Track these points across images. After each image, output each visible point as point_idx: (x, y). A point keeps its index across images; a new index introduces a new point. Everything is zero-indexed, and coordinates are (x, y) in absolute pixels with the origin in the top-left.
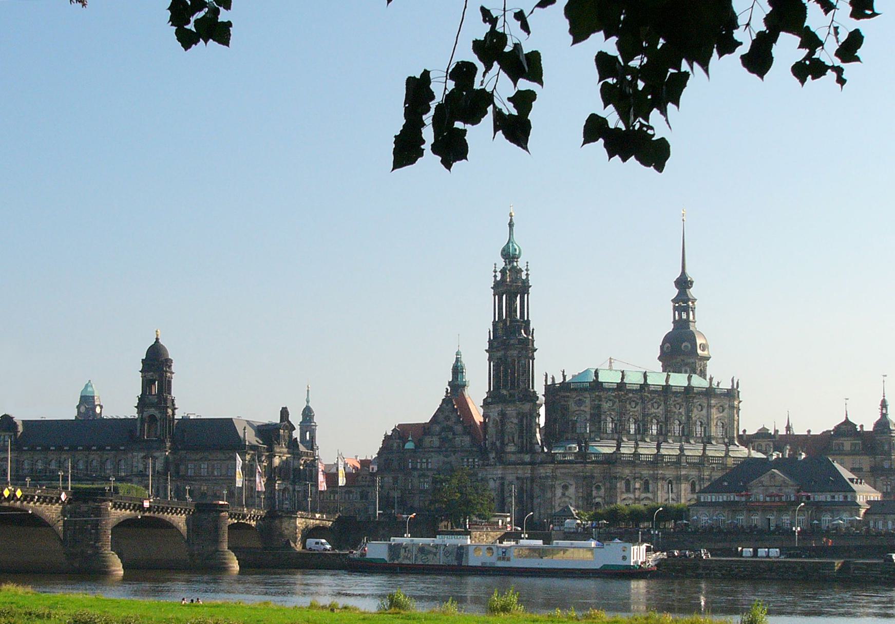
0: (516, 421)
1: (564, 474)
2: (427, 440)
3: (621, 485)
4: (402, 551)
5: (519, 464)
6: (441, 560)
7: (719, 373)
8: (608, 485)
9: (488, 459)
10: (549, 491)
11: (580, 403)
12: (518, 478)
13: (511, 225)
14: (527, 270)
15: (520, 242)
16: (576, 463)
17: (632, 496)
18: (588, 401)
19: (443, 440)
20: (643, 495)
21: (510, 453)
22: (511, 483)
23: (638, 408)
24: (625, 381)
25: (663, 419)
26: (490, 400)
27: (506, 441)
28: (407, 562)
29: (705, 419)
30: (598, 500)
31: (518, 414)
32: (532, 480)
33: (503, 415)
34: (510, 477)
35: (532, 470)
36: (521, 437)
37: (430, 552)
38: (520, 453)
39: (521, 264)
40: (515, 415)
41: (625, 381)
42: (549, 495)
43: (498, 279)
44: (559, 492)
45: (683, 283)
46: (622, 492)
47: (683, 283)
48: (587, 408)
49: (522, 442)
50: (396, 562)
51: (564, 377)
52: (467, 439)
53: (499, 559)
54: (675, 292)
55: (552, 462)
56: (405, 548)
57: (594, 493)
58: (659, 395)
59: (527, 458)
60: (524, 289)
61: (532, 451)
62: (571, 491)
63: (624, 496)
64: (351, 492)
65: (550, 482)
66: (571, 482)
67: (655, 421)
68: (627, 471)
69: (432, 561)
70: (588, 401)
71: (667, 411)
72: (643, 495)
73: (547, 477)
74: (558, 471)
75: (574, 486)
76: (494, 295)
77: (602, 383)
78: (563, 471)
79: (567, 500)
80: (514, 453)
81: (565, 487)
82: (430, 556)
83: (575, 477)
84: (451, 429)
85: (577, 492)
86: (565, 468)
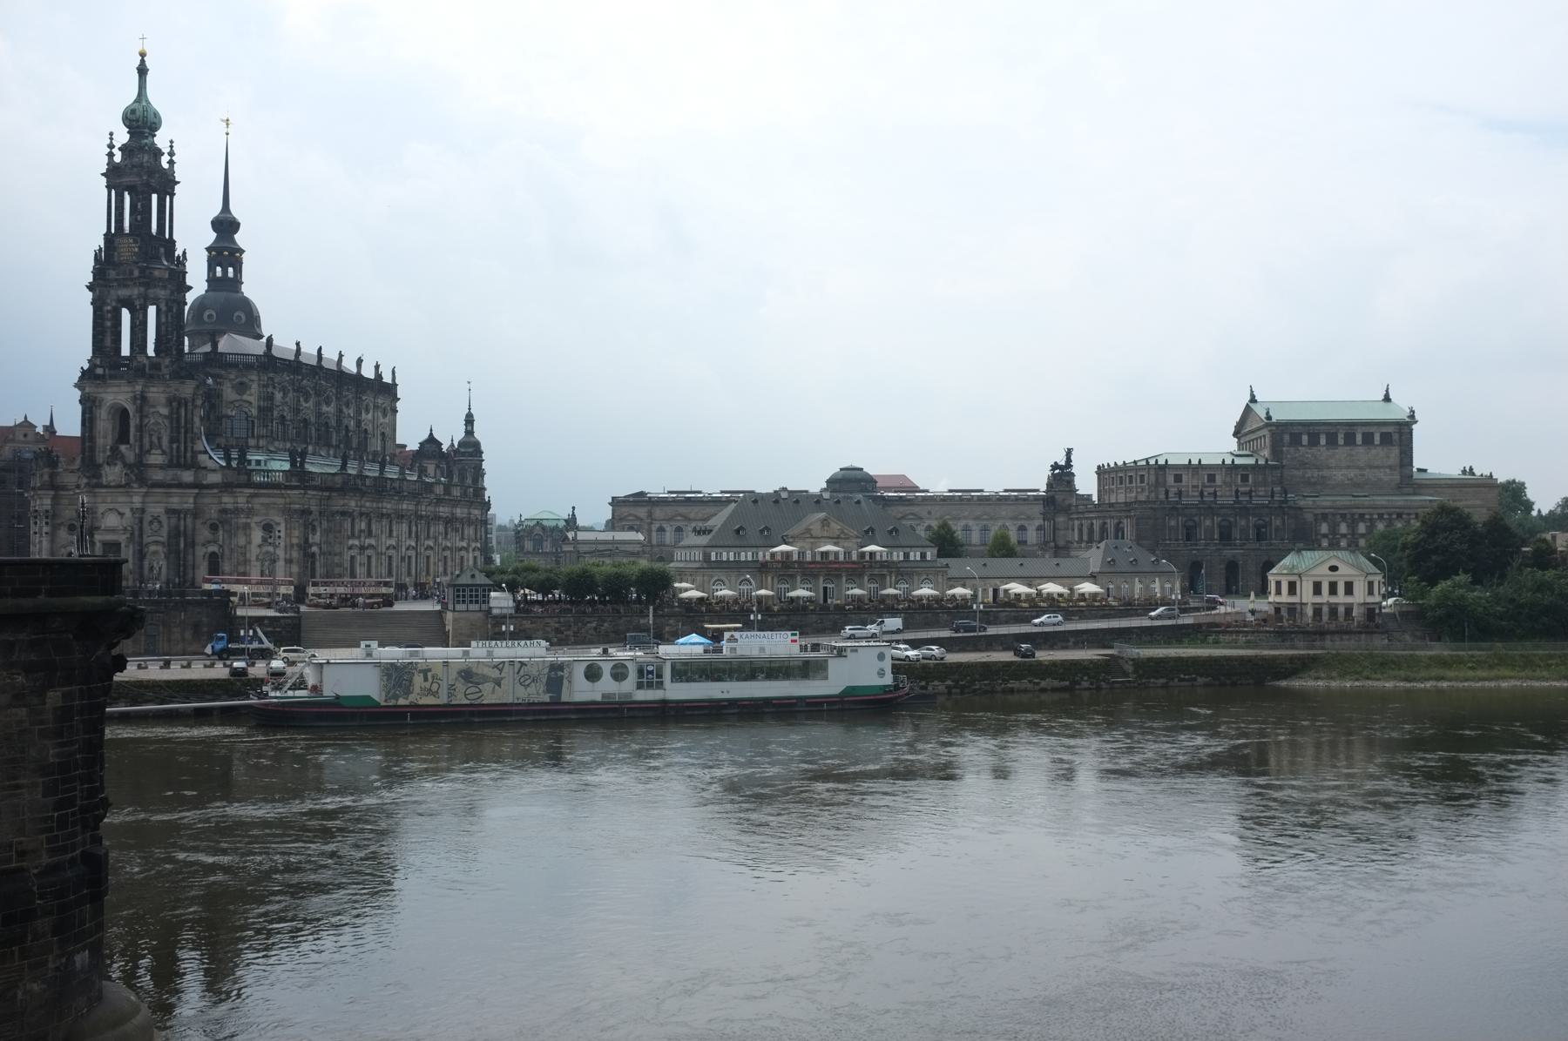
0: (164, 411)
3: (347, 525)
4: (418, 680)
5: (170, 486)
6: (509, 693)
10: (241, 532)
11: (242, 388)
12: (170, 512)
13: (142, 71)
14: (171, 154)
15: (157, 99)
16: (287, 487)
18: (255, 386)
21: (155, 466)
22: (156, 519)
23: (310, 404)
25: (333, 422)
27: (147, 447)
28: (429, 700)
31: (170, 401)
32: (196, 513)
33: (142, 400)
35: (196, 496)
36: (172, 441)
37: (486, 679)
40: (163, 401)
42: (242, 541)
43: (118, 158)
45: (225, 226)
47: (225, 226)
48: (252, 396)
50: (402, 702)
53: (640, 686)
55: (249, 484)
56: (425, 672)
59: (188, 476)
60: (167, 184)
61: (194, 465)
66: (277, 519)
68: (353, 503)
69: (490, 695)
70: (255, 386)
74: (256, 500)
76: (109, 187)
79: (271, 549)
80: (161, 467)
82: (487, 687)
83: (288, 512)
86: (268, 496)
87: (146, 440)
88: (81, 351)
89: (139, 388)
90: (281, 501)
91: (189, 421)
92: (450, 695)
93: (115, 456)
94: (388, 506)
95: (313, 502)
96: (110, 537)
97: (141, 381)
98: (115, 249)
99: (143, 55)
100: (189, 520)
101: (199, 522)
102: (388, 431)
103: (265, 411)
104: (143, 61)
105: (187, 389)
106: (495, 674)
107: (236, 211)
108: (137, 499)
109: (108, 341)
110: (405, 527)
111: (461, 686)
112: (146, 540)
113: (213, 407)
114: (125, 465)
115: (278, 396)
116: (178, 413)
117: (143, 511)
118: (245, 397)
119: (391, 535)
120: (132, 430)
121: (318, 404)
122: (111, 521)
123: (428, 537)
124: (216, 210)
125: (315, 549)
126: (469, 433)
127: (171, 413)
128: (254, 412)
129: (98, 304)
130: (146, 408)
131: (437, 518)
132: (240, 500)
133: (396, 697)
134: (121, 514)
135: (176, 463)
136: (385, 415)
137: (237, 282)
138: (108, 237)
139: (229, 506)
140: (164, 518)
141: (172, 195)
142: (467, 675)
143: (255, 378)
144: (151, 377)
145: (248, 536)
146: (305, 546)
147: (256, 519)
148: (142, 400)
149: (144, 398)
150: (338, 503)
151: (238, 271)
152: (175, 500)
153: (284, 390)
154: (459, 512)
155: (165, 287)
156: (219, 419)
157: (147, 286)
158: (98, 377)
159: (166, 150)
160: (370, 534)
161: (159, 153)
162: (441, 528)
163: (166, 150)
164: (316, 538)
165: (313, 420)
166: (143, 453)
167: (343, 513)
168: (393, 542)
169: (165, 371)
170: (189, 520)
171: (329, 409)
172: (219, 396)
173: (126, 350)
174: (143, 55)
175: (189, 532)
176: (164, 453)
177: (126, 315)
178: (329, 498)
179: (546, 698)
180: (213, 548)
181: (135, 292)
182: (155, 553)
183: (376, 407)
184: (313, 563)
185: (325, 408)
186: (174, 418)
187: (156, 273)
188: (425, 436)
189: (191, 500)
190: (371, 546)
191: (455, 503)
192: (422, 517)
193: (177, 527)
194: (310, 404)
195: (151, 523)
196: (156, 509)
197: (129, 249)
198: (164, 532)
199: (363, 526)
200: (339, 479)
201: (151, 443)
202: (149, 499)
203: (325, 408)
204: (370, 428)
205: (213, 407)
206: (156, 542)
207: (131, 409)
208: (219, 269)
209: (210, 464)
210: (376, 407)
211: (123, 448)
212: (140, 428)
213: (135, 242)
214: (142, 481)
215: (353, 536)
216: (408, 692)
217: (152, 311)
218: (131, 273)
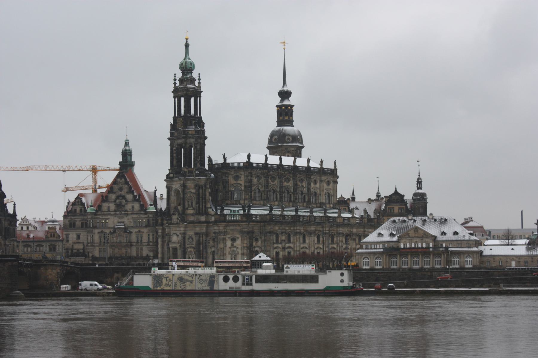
1: (233, 230)
2: (105, 206)
5: (196, 223)
7: (311, 157)
8: (263, 238)
9: (171, 220)
10: (221, 242)
11: (237, 178)
12: (196, 234)
13: (187, 46)
14: (199, 79)
15: (193, 57)
16: (242, 222)
17: (280, 246)
18: (243, 177)
19: (119, 207)
20: (287, 245)
21: (190, 214)
22: (191, 237)
23: (276, 182)
25: (292, 190)
26: (171, 175)
27: (187, 206)
29: (318, 190)
30: (257, 249)
32: (207, 234)
33: (184, 186)
34: (190, 233)
35: (207, 227)
36: (196, 204)
37: (187, 281)
39: (195, 75)
40: (193, 186)
41: (268, 162)
42: (222, 245)
43: (177, 85)
44: (229, 243)
48: (242, 181)
49: (199, 207)
51: (225, 159)
52: (137, 206)
55: (225, 221)
57: (254, 243)
58: (290, 173)
59: (203, 218)
60: (197, 93)
62: (238, 242)
63: (275, 245)
64: (42, 246)
65: (222, 237)
66: (238, 236)
67: (286, 192)
68: (277, 228)
69: (189, 287)
70: (243, 177)
71: (296, 185)
72: (287, 245)
73: (220, 233)
74: (228, 228)
75: (240, 238)
76: (174, 97)
77: (253, 163)
78: (232, 228)
79: (235, 249)
80: (193, 215)
81: (234, 240)
82: (188, 284)
83: (241, 232)
84: (124, 197)
85: (242, 243)
86: (233, 226)
87: (186, 204)
90: (239, 228)
92: (175, 286)
96: (174, 245)
98: (177, 123)
99: (187, 39)
100: (204, 237)
101: (208, 238)
106: (190, 279)
108: (182, 229)
111: (178, 283)
112: (187, 246)
115: (255, 180)
121: (281, 182)
122: (175, 238)
128: (243, 188)
131: (339, 234)
132: (221, 228)
133: (157, 287)
134: (178, 236)
135: (199, 212)
138: (175, 119)
139: (217, 231)
140: (194, 236)
141: (200, 97)
142: (181, 279)
143: (243, 173)
147: (228, 236)
150: (268, 228)
152: (197, 229)
153: (258, 177)
154: (355, 230)
155: (193, 138)
158: (171, 178)
159: (197, 78)
160: (289, 241)
163: (197, 78)
165: (278, 190)
166: (184, 209)
170: (204, 237)
172: (227, 182)
176: (194, 209)
178: (264, 226)
179: (208, 288)
180: (213, 249)
182: (191, 251)
183: (321, 181)
188: (393, 192)
189: (205, 229)
190: (290, 247)
192: (326, 233)
194: (276, 182)
195: (189, 239)
196: (190, 233)
198: (194, 243)
200: (268, 217)
201: (189, 205)
202: (188, 229)
203: (285, 184)
206: (191, 247)
207: (180, 190)
211: (179, 207)
215: (277, 242)
216: (161, 285)
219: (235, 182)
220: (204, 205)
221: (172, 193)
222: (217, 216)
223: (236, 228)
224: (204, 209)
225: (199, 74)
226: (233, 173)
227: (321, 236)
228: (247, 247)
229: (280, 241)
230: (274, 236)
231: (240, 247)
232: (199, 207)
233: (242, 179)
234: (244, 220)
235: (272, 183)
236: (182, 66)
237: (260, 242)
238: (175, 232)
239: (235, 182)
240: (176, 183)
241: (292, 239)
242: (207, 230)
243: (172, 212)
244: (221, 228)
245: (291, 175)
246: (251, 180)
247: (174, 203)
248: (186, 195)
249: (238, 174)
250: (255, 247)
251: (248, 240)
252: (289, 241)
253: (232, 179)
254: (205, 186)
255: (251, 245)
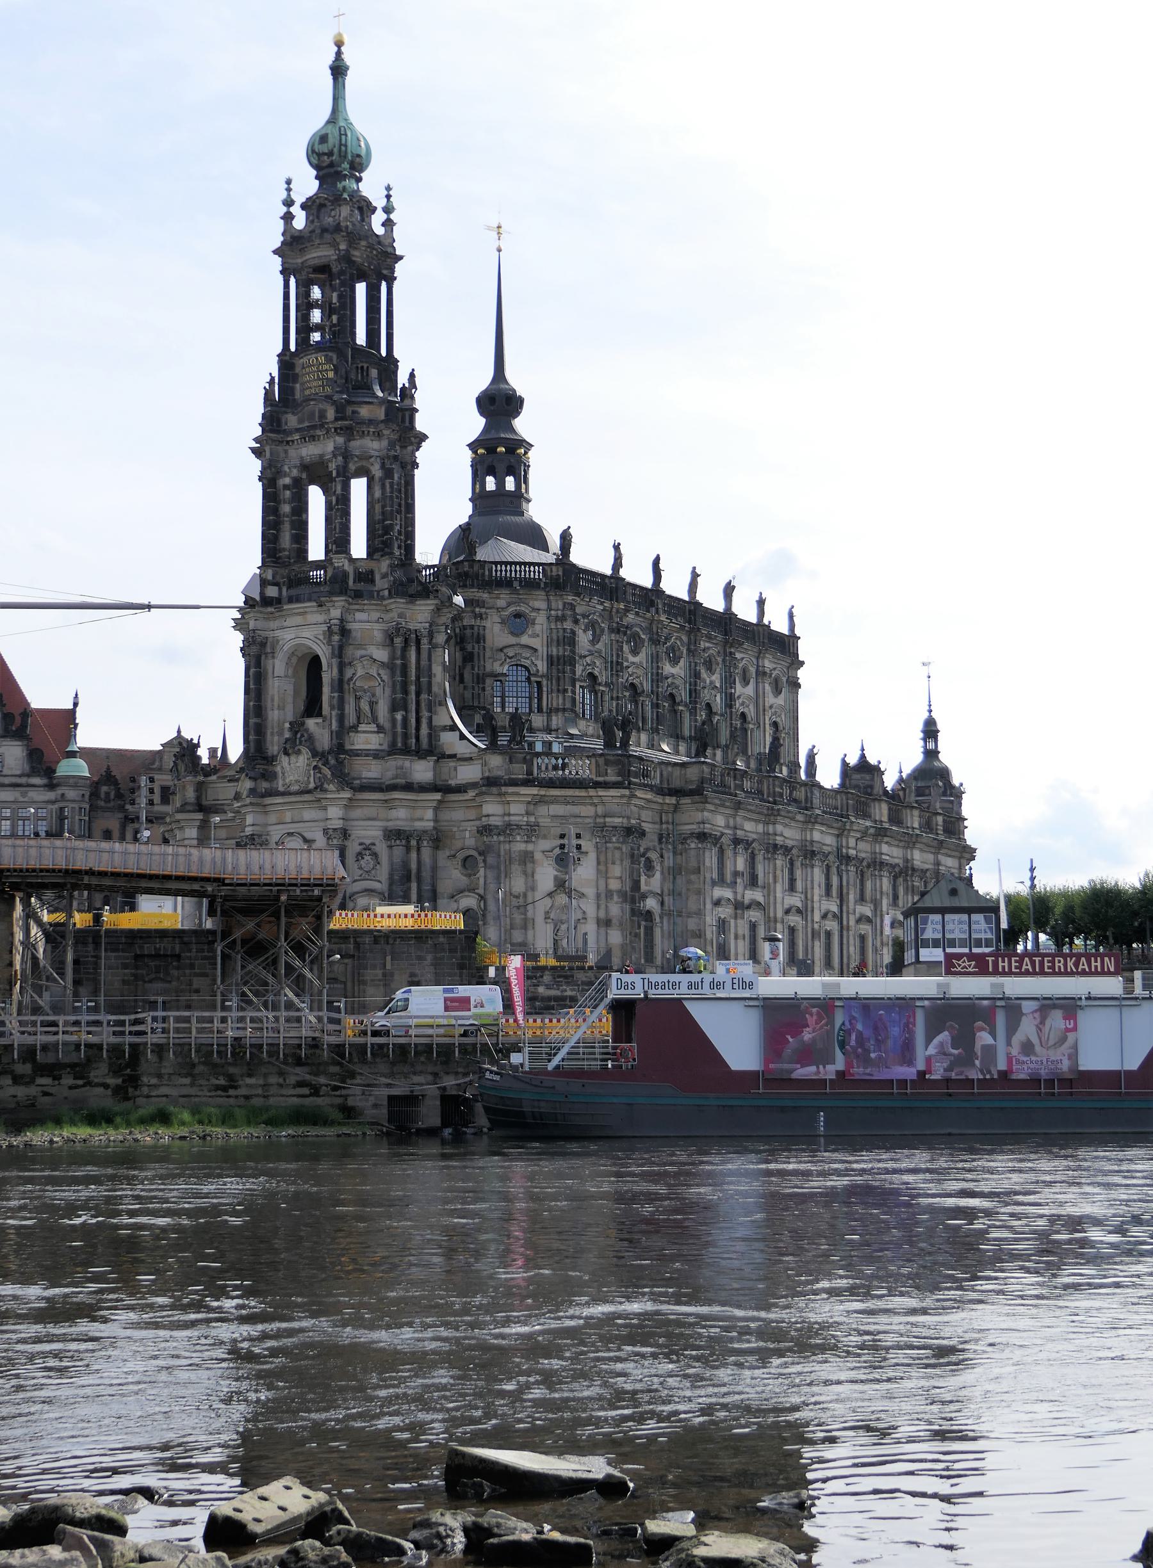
0: (382, 655)
3: (710, 859)
5: (393, 788)
10: (516, 869)
11: (518, 622)
12: (394, 835)
13: (338, 70)
14: (388, 210)
15: (363, 120)
16: (597, 785)
17: (728, 894)
21: (367, 753)
22: (368, 849)
24: (623, 573)
25: (683, 695)
27: (351, 719)
31: (390, 638)
32: (438, 839)
33: (342, 633)
36: (394, 708)
38: (393, 751)
39: (370, 187)
40: (378, 636)
41: (623, 573)
42: (518, 884)
43: (300, 221)
45: (500, 404)
46: (714, 883)
47: (500, 404)
48: (537, 637)
54: (476, 424)
57: (643, 878)
59: (422, 771)
60: (379, 263)
61: (432, 751)
62: (584, 873)
65: (519, 846)
68: (720, 821)
70: (541, 619)
73: (508, 829)
74: (543, 810)
75: (592, 856)
80: (376, 755)
83: (601, 830)
85: (602, 870)
86: (566, 802)
88: (245, 559)
89: (336, 613)
90: (587, 811)
91: (424, 672)
93: (297, 738)
94: (788, 833)
95: (646, 815)
97: (340, 601)
98: (295, 378)
99: (339, 44)
100: (426, 853)
101: (442, 855)
102: (783, 720)
103: (562, 662)
104: (339, 54)
105: (420, 614)
107: (516, 379)
109: (286, 540)
110: (818, 874)
113: (468, 658)
114: (315, 753)
115: (584, 639)
116: (404, 657)
117: (345, 833)
118: (525, 640)
119: (792, 888)
120: (326, 690)
121: (655, 659)
123: (862, 899)
124: (483, 379)
125: (651, 903)
126: (931, 754)
127: (393, 657)
128: (542, 666)
129: (269, 480)
130: (349, 652)
131: (877, 864)
132: (515, 808)
136: (777, 691)
137: (518, 499)
138: (286, 361)
139: (496, 821)
141: (390, 280)
143: (542, 605)
144: (358, 595)
145: (530, 875)
146: (633, 894)
147: (545, 844)
148: (342, 633)
149: (344, 632)
150: (692, 817)
151: (522, 479)
155: (379, 435)
156: (480, 679)
157: (349, 432)
159: (379, 202)
160: (753, 882)
161: (365, 208)
162: (886, 884)
164: (653, 883)
165: (647, 686)
166: (343, 730)
167: (702, 837)
168: (796, 901)
169: (381, 584)
170: (426, 853)
171: (676, 671)
172: (480, 639)
173: (316, 550)
174: (339, 44)
175: (426, 874)
176: (380, 729)
177: (316, 498)
178: (676, 808)
181: (327, 447)
184: (649, 932)
185: (668, 669)
186: (398, 669)
187: (364, 412)
189: (429, 814)
191: (910, 841)
192: (848, 858)
193: (405, 865)
195: (360, 855)
196: (368, 832)
197: (318, 371)
198: (383, 872)
199: (741, 864)
201: (359, 711)
202: (357, 813)
203: (668, 669)
204: (751, 712)
205: (468, 658)
207: (323, 652)
208: (490, 483)
209: (461, 749)
210: (761, 674)
211: (311, 723)
212: (340, 685)
213: (329, 360)
214: (344, 779)
215: (721, 881)
217: (359, 488)
218: (323, 414)
219: (513, 640)
220: (425, 714)
221: (278, 666)
222: (496, 761)
223: (575, 810)
224: (424, 730)
225: (388, 188)
226: (501, 603)
227: (834, 870)
228: (623, 894)
229: (729, 877)
230: (715, 850)
231: (590, 892)
232: (405, 720)
233: (538, 628)
234: (612, 778)
235: (631, 659)
236: (324, 148)
237: (658, 875)
238: (292, 828)
239: (513, 640)
240: (298, 620)
241: (760, 869)
242: (436, 820)
243: (273, 745)
244: (517, 808)
245: (685, 638)
246: (573, 633)
247: (281, 708)
248: (348, 673)
249: (523, 608)
250: (644, 897)
251: (627, 863)
252: (753, 882)
253: (497, 628)
254: (431, 635)
255: (636, 885)
